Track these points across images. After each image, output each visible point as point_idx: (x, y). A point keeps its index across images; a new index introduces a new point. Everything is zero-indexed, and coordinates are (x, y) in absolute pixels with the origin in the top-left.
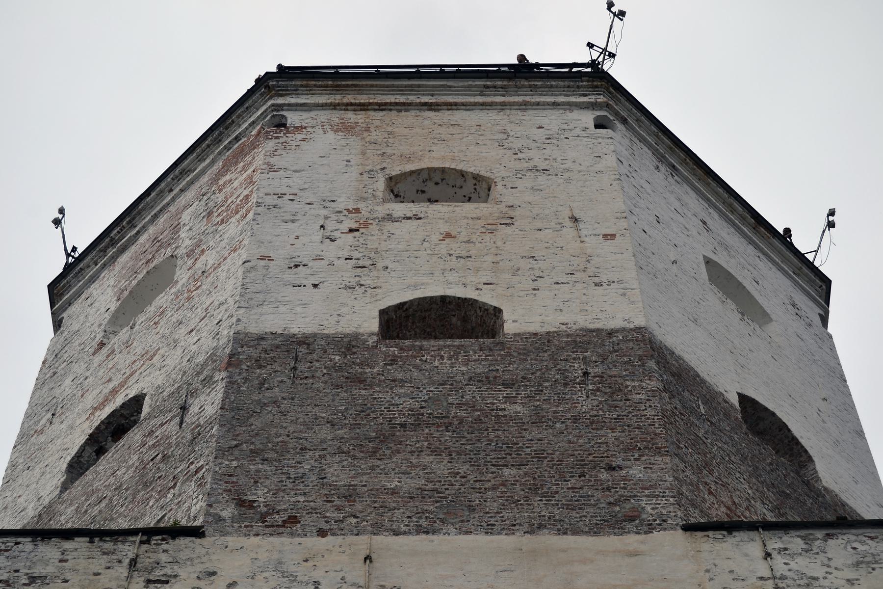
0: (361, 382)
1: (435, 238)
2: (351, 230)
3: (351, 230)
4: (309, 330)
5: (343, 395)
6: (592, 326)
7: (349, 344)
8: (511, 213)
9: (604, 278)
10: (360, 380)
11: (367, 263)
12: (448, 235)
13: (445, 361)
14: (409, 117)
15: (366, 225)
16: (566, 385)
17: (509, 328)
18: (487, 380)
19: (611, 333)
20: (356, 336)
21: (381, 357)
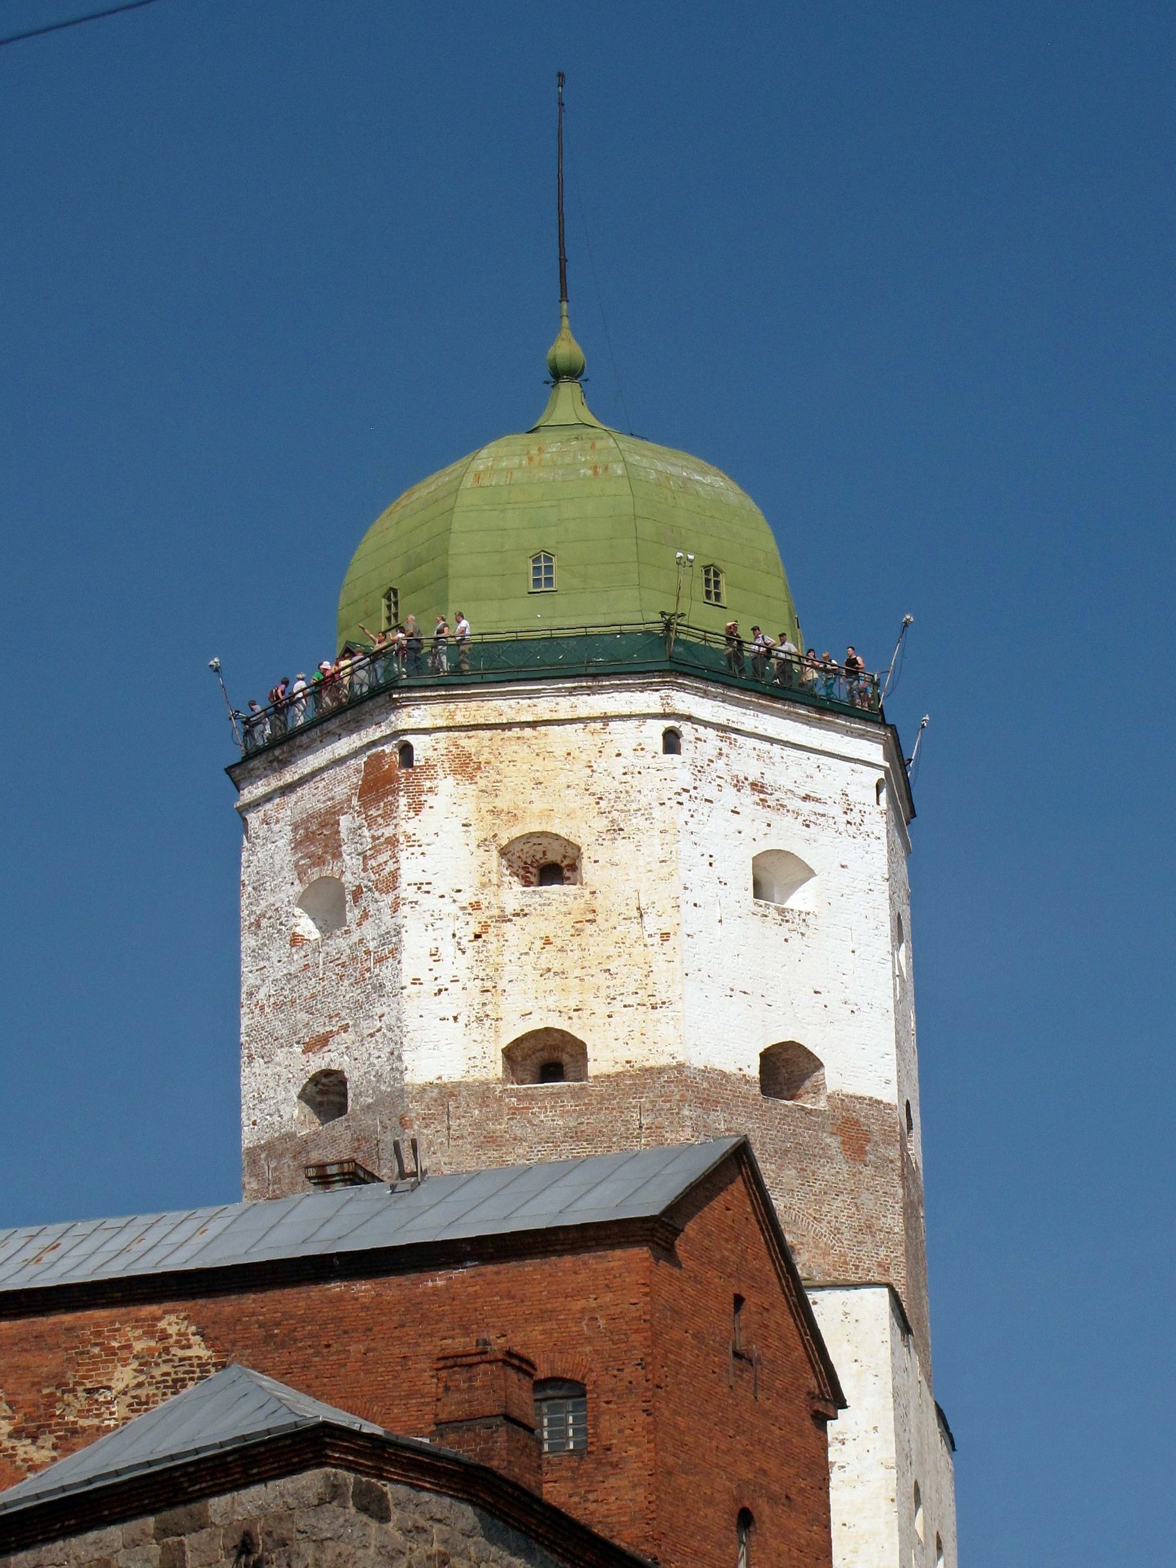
0: (494, 1142)
1: (539, 944)
2: (477, 936)
3: (477, 936)
4: (457, 1078)
5: (484, 1158)
6: (647, 1065)
7: (482, 1093)
8: (596, 904)
9: (661, 996)
10: (492, 1140)
11: (489, 984)
12: (548, 942)
13: (552, 1108)
14: (511, 745)
15: (486, 926)
16: (627, 1138)
17: (593, 1069)
18: (575, 1135)
19: (661, 1071)
20: (485, 1084)
21: (505, 1110)
